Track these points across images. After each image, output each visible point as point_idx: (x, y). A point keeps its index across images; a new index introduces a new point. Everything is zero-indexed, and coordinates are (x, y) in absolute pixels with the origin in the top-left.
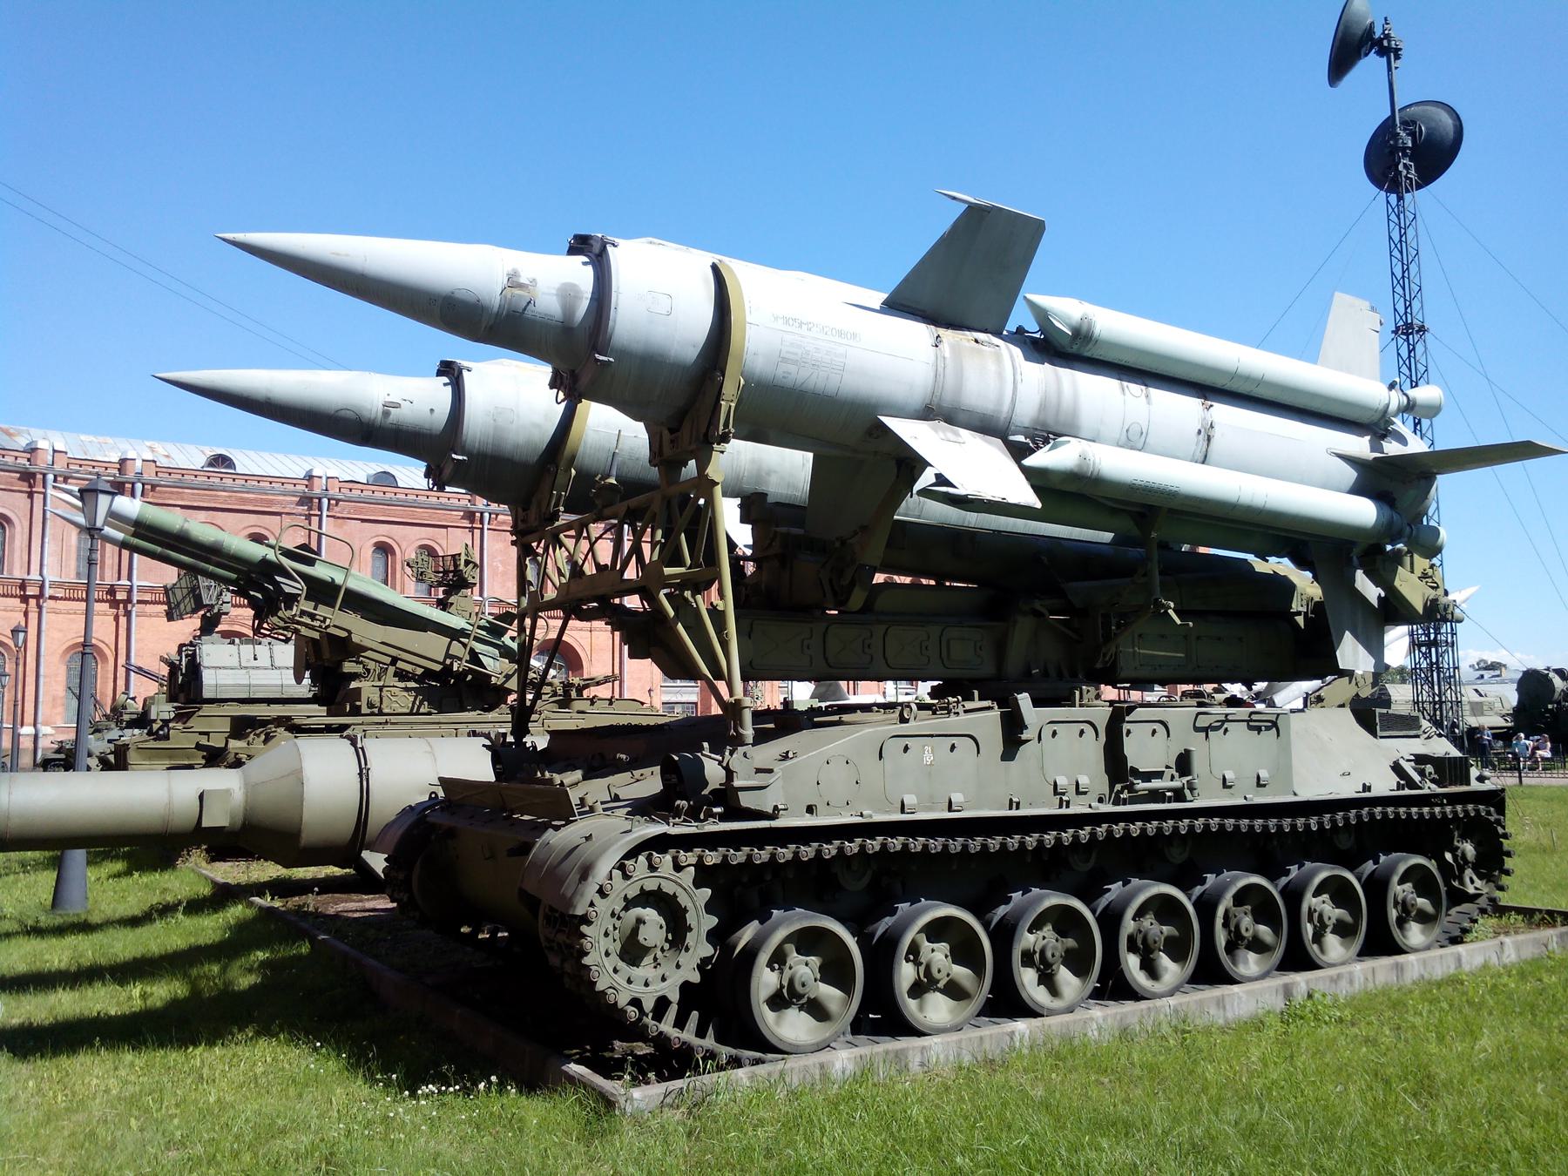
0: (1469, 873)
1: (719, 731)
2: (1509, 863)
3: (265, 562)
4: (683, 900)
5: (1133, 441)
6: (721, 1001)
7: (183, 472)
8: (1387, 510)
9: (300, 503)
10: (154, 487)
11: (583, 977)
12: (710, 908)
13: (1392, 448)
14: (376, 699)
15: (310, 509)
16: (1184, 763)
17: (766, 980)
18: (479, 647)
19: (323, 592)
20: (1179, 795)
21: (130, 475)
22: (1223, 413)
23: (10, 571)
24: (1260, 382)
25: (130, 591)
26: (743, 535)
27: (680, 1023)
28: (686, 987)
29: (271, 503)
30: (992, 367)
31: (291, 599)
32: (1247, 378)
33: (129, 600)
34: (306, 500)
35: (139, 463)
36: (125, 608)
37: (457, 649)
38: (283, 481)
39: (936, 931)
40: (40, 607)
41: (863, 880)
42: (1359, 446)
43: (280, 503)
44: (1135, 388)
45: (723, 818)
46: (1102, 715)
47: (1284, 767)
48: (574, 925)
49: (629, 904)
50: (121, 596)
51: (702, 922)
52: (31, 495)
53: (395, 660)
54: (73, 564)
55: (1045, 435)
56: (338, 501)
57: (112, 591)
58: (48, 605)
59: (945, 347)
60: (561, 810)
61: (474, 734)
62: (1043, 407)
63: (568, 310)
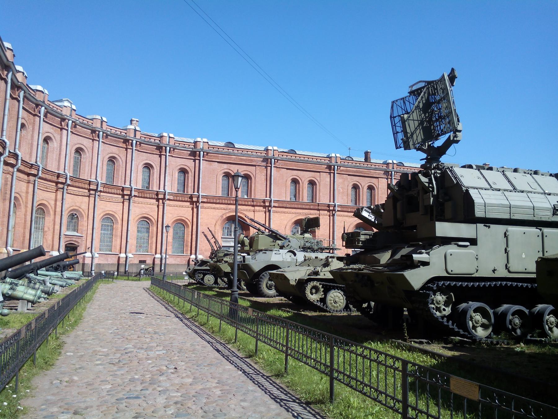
9: (263, 161)
15: (267, 163)
23: (152, 188)
25: (198, 197)
29: (252, 161)
33: (198, 201)
35: (202, 144)
36: (196, 204)
38: (257, 151)
40: (164, 203)
43: (255, 161)
50: (195, 199)
52: (160, 156)
54: (176, 185)
56: (278, 160)
57: (191, 197)
58: (167, 202)
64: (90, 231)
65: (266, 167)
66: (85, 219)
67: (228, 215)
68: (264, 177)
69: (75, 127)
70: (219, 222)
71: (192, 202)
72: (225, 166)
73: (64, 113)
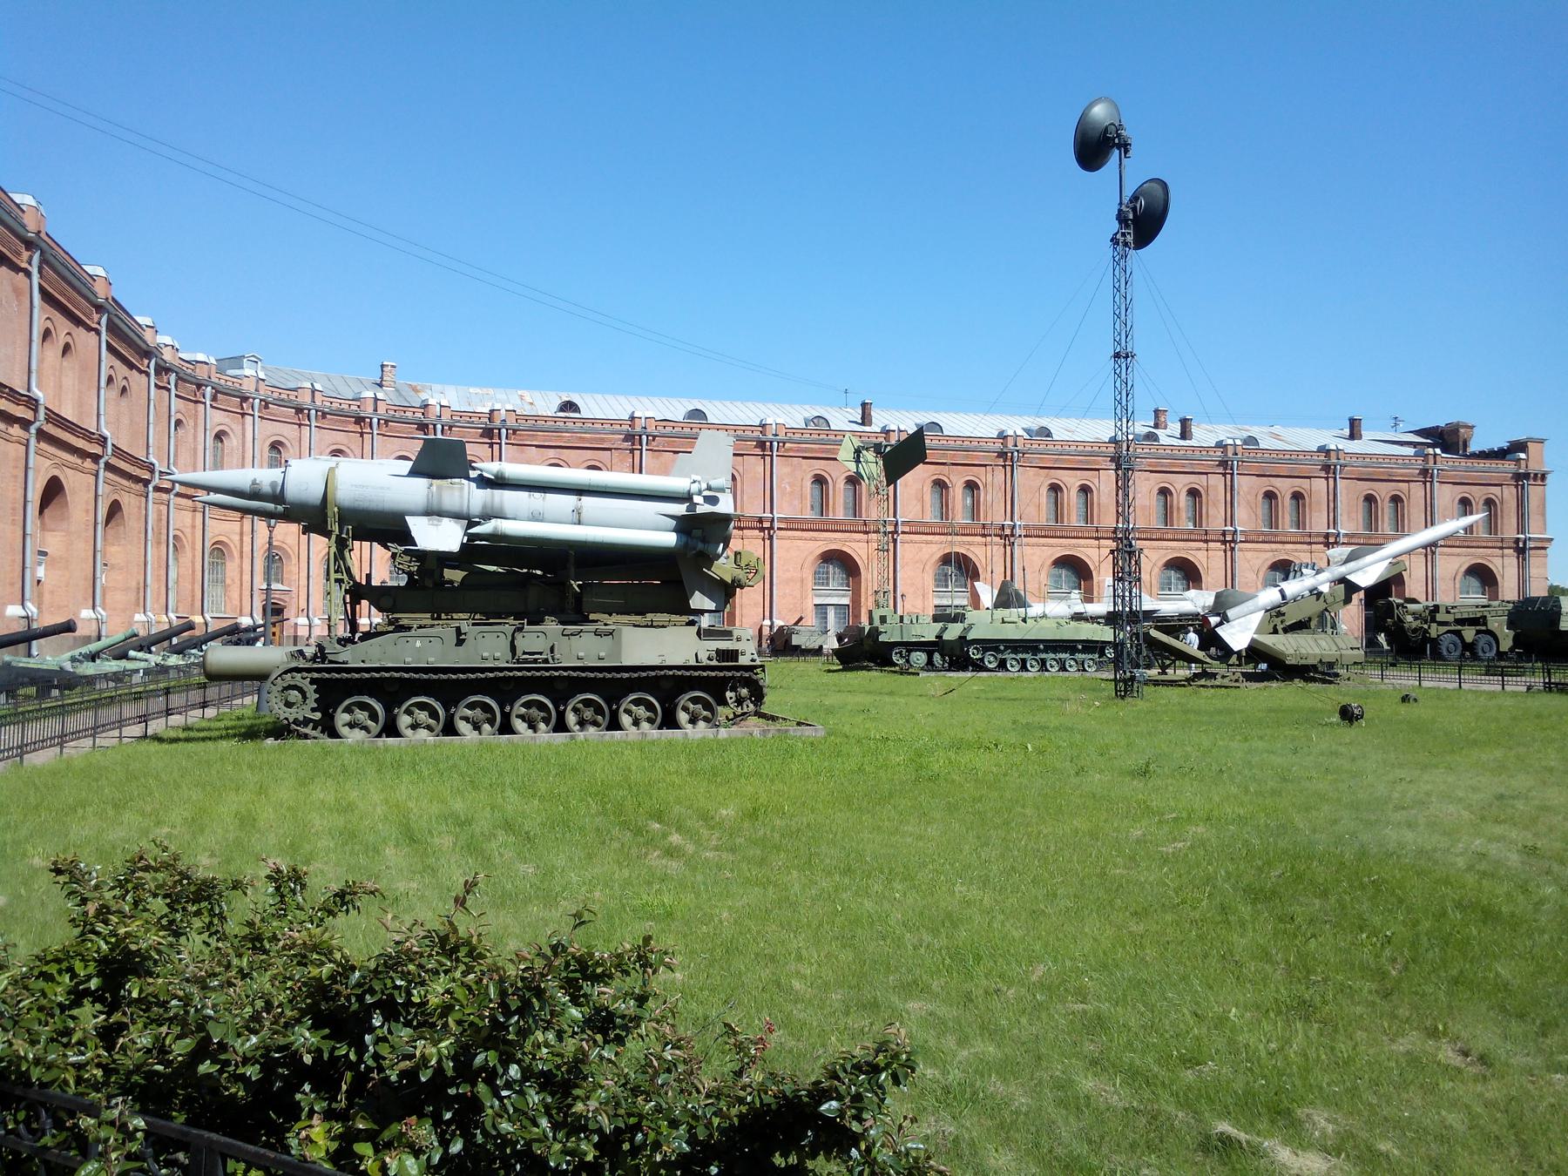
5: (536, 517)
7: (537, 418)
8: (684, 539)
9: (625, 440)
16: (552, 650)
20: (546, 661)
21: (497, 423)
22: (587, 501)
29: (603, 440)
30: (457, 493)
34: (629, 437)
38: (612, 422)
51: (441, 712)
59: (434, 488)
62: (484, 507)
65: (632, 451)
69: (266, 407)
73: (244, 387)
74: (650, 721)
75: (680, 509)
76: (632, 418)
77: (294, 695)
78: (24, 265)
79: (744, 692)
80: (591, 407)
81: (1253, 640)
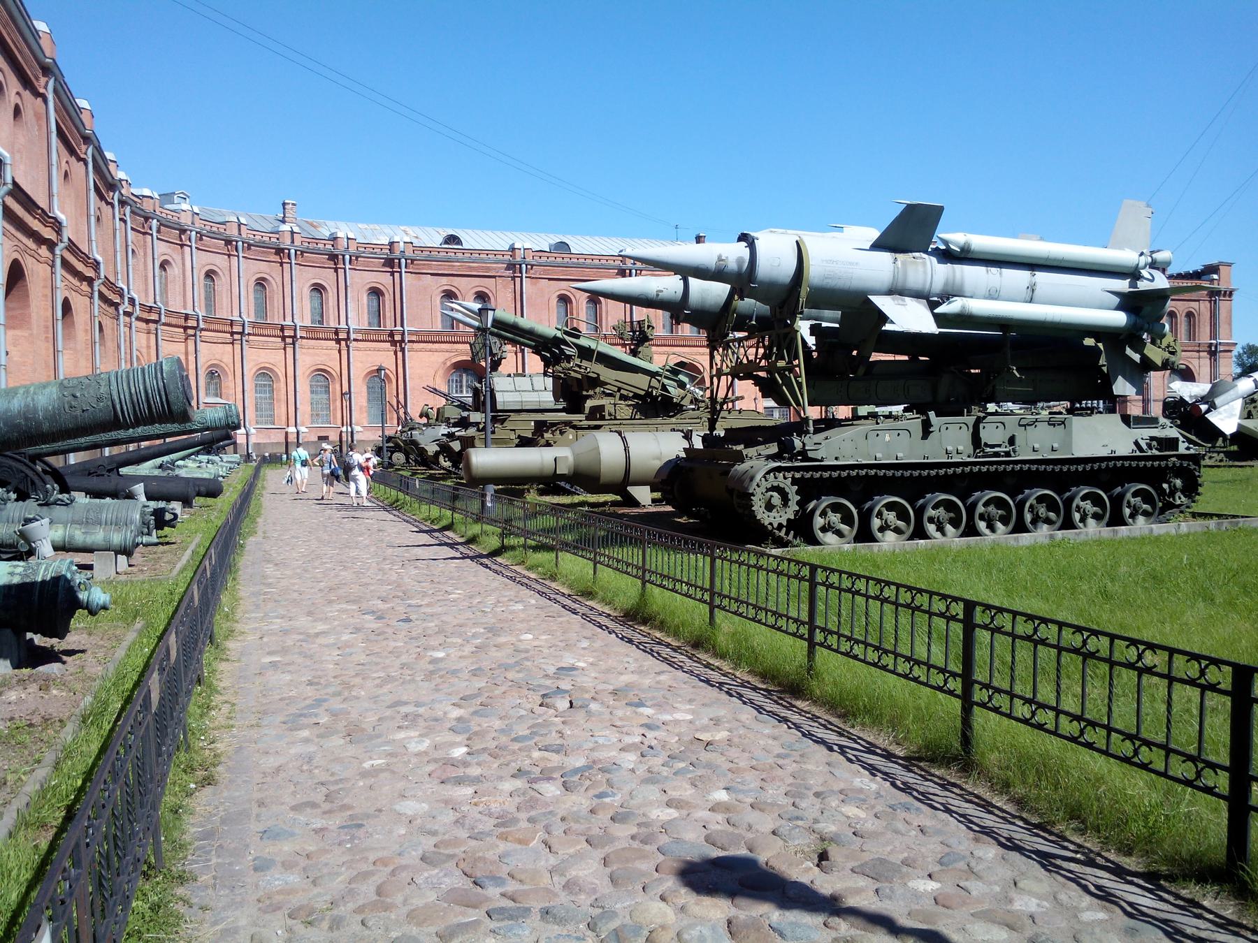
0: (1179, 494)
1: (800, 427)
2: (1200, 490)
3: (555, 338)
4: (787, 490)
5: (992, 295)
6: (802, 528)
7: (431, 249)
8: (1133, 317)
9: (507, 269)
10: (413, 261)
11: (752, 515)
12: (797, 493)
13: (1143, 285)
14: (612, 411)
16: (1012, 441)
17: (819, 522)
18: (666, 382)
19: (586, 353)
20: (1008, 454)
21: (397, 253)
22: (1042, 277)
23: (328, 323)
24: (1063, 260)
25: (403, 334)
26: (811, 341)
27: (787, 534)
28: (789, 520)
29: (488, 269)
30: (921, 269)
31: (569, 359)
32: (1055, 260)
33: (403, 341)
34: (511, 266)
35: (402, 244)
37: (654, 383)
38: (496, 252)
39: (890, 507)
40: (348, 347)
41: (859, 488)
42: (1123, 285)
44: (994, 270)
45: (802, 461)
46: (971, 420)
47: (1068, 442)
48: (748, 496)
49: (768, 490)
50: (398, 338)
53: (619, 389)
54: (366, 316)
55: (946, 296)
57: (392, 334)
58: (353, 344)
59: (899, 263)
60: (740, 458)
61: (673, 430)
62: (946, 284)
63: (740, 267)
64: (240, 396)
65: (513, 278)
66: (231, 377)
67: (454, 361)
68: (511, 296)
69: (201, 239)
70: (441, 372)
71: (394, 343)
72: (444, 280)
73: (182, 221)
74: (1097, 517)
75: (1123, 285)
76: (513, 249)
77: (776, 499)
78: (42, 90)
79: (1178, 482)
80: (471, 240)
81: (1240, 426)
